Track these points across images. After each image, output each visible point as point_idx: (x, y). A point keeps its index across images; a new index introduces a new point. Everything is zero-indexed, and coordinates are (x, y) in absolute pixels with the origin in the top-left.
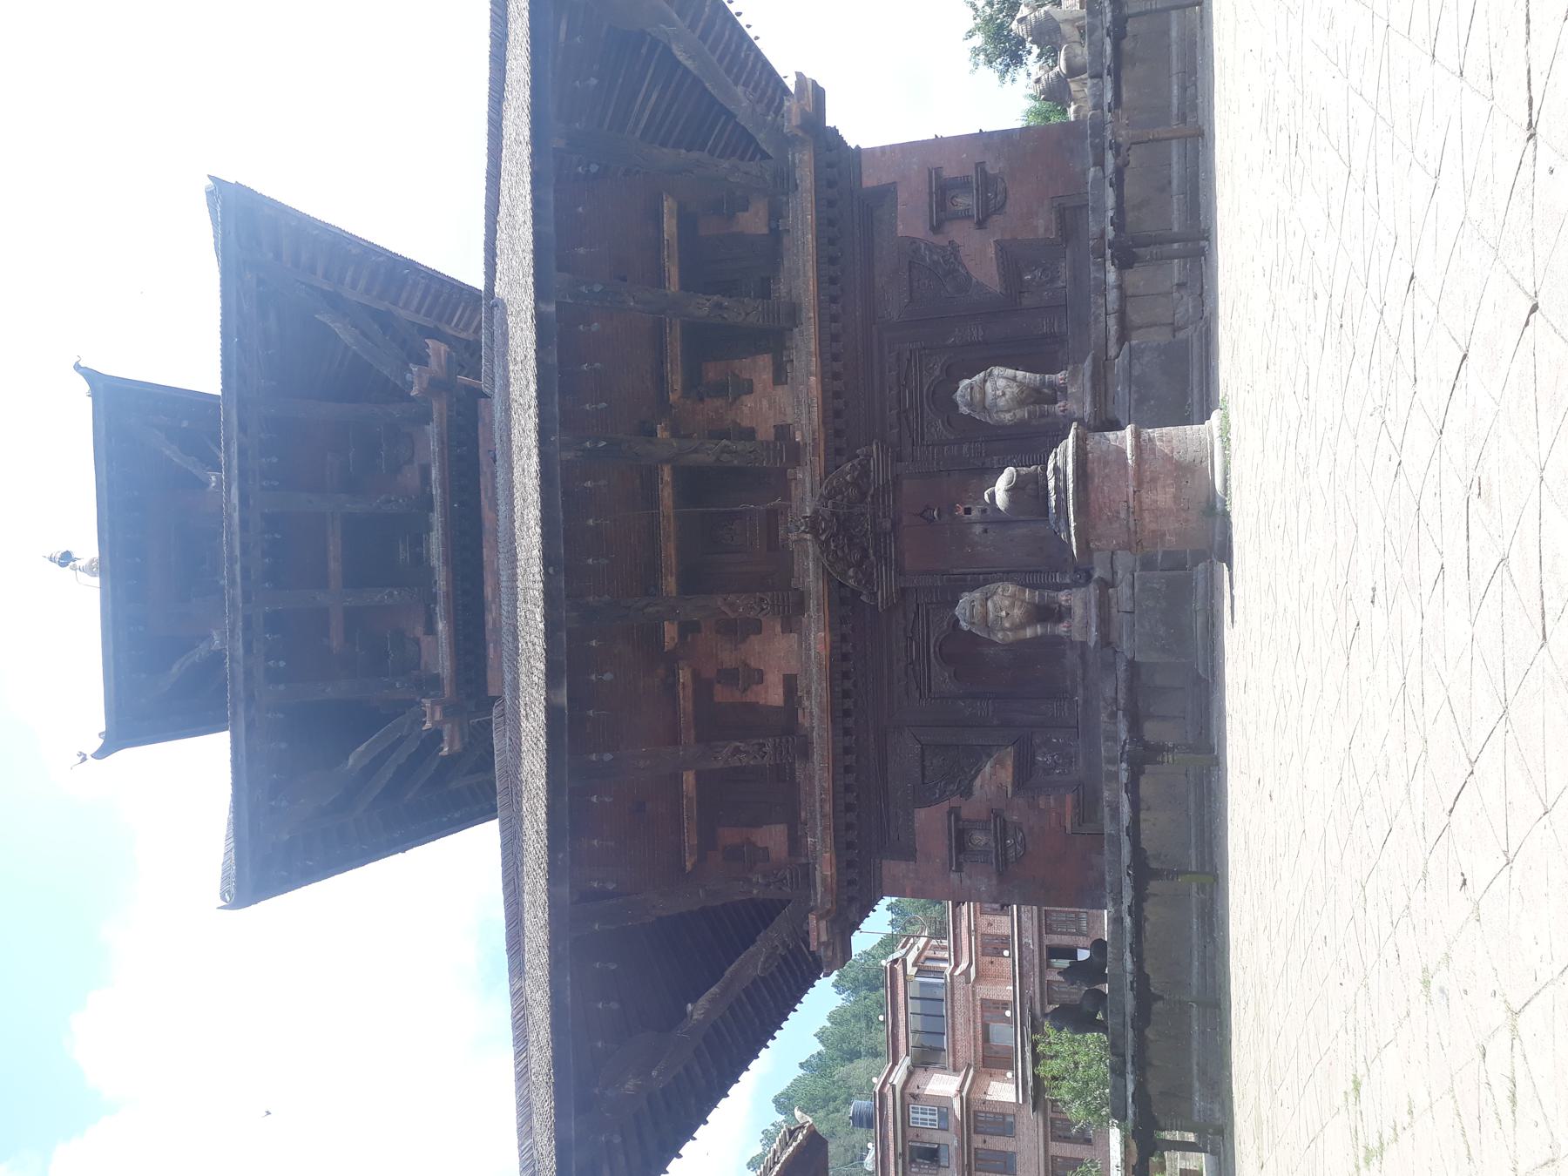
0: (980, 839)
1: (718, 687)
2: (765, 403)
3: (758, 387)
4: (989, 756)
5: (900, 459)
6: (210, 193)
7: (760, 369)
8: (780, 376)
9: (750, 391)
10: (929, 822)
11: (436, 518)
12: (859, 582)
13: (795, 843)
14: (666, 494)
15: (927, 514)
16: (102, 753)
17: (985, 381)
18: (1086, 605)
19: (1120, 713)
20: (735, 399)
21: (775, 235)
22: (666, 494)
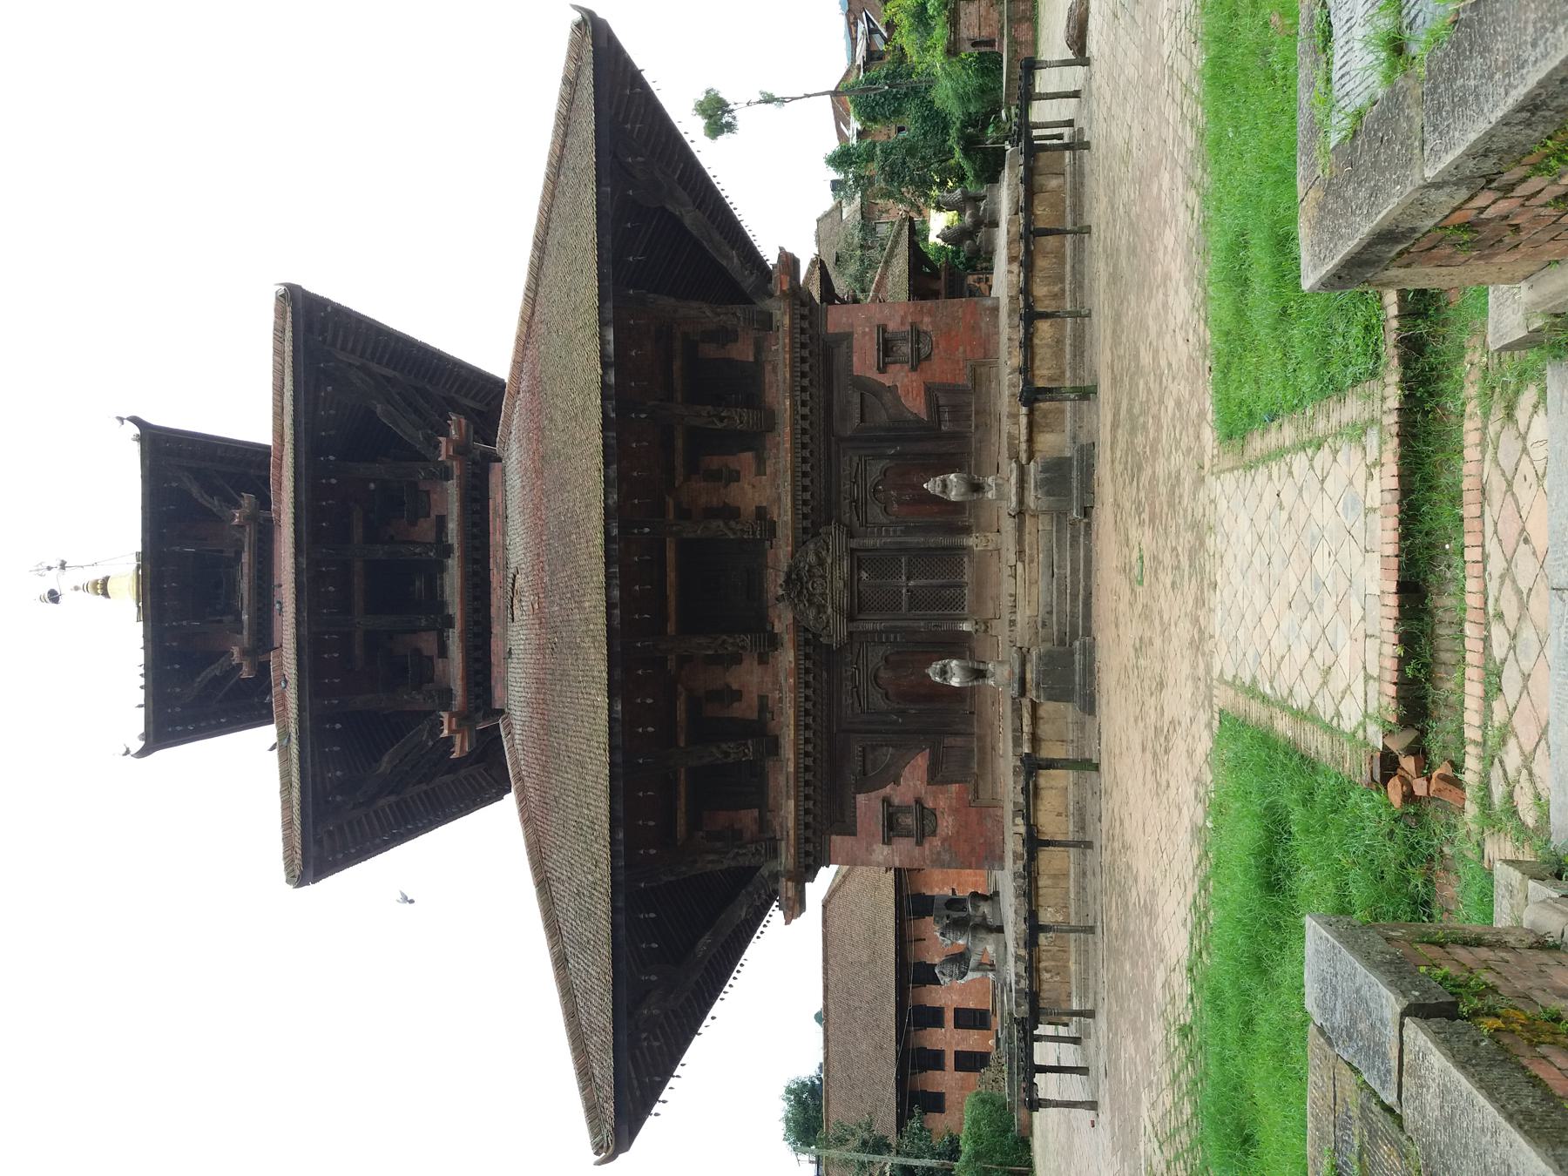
0: (909, 821)
6: (281, 298)
8: (761, 471)
10: (867, 806)
11: (454, 565)
13: (763, 823)
14: (671, 555)
16: (143, 753)
21: (758, 364)
22: (671, 555)
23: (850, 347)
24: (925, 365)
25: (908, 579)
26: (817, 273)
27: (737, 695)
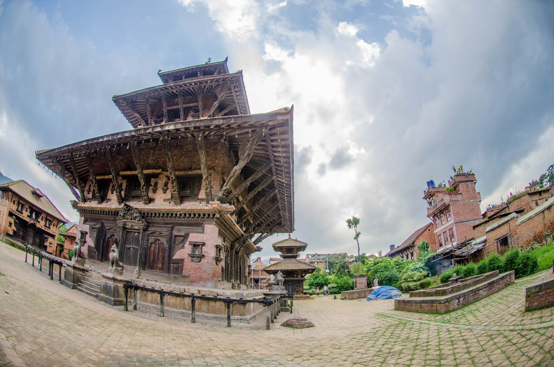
8: (164, 200)
21: (199, 199)
23: (199, 233)
24: (190, 258)
25: (134, 248)
26: (298, 245)
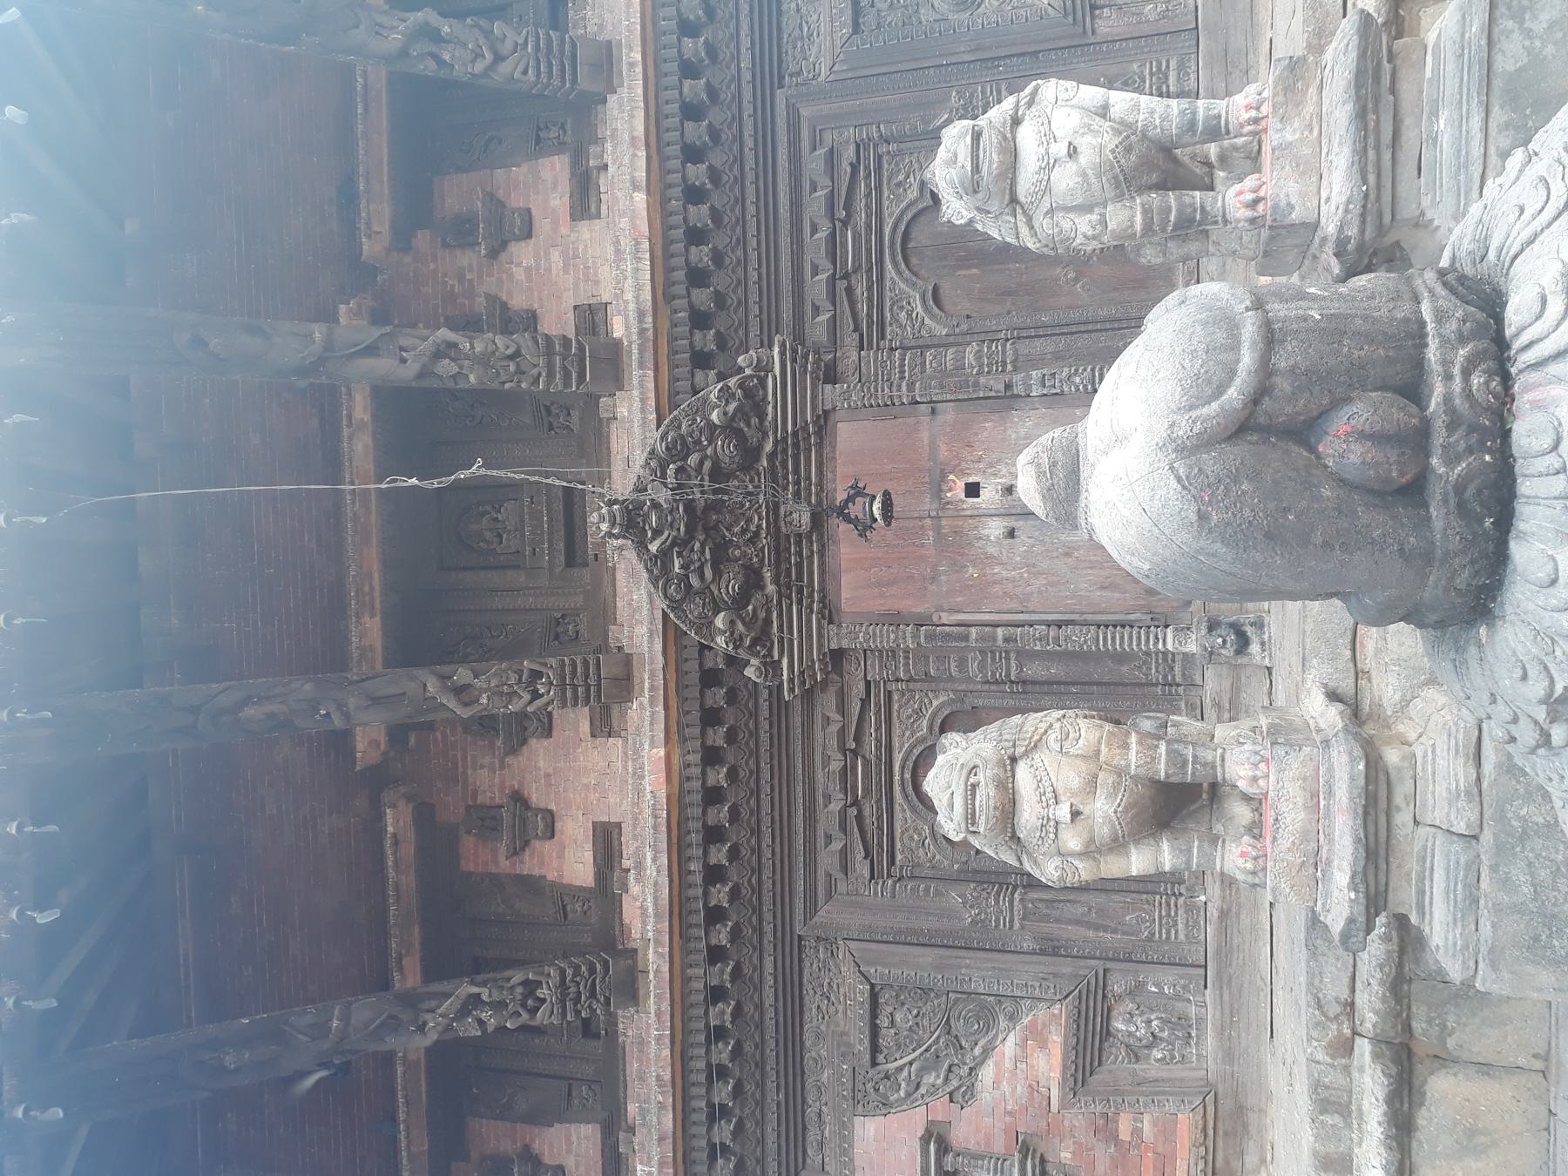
1: (468, 843)
2: (556, 256)
3: (542, 225)
4: (1013, 1018)
5: (831, 375)
7: (544, 184)
9: (528, 234)
12: (737, 642)
15: (855, 510)
17: (1016, 121)
18: (1315, 800)
19: (1364, 1047)
20: (494, 254)
27: (529, 822)
